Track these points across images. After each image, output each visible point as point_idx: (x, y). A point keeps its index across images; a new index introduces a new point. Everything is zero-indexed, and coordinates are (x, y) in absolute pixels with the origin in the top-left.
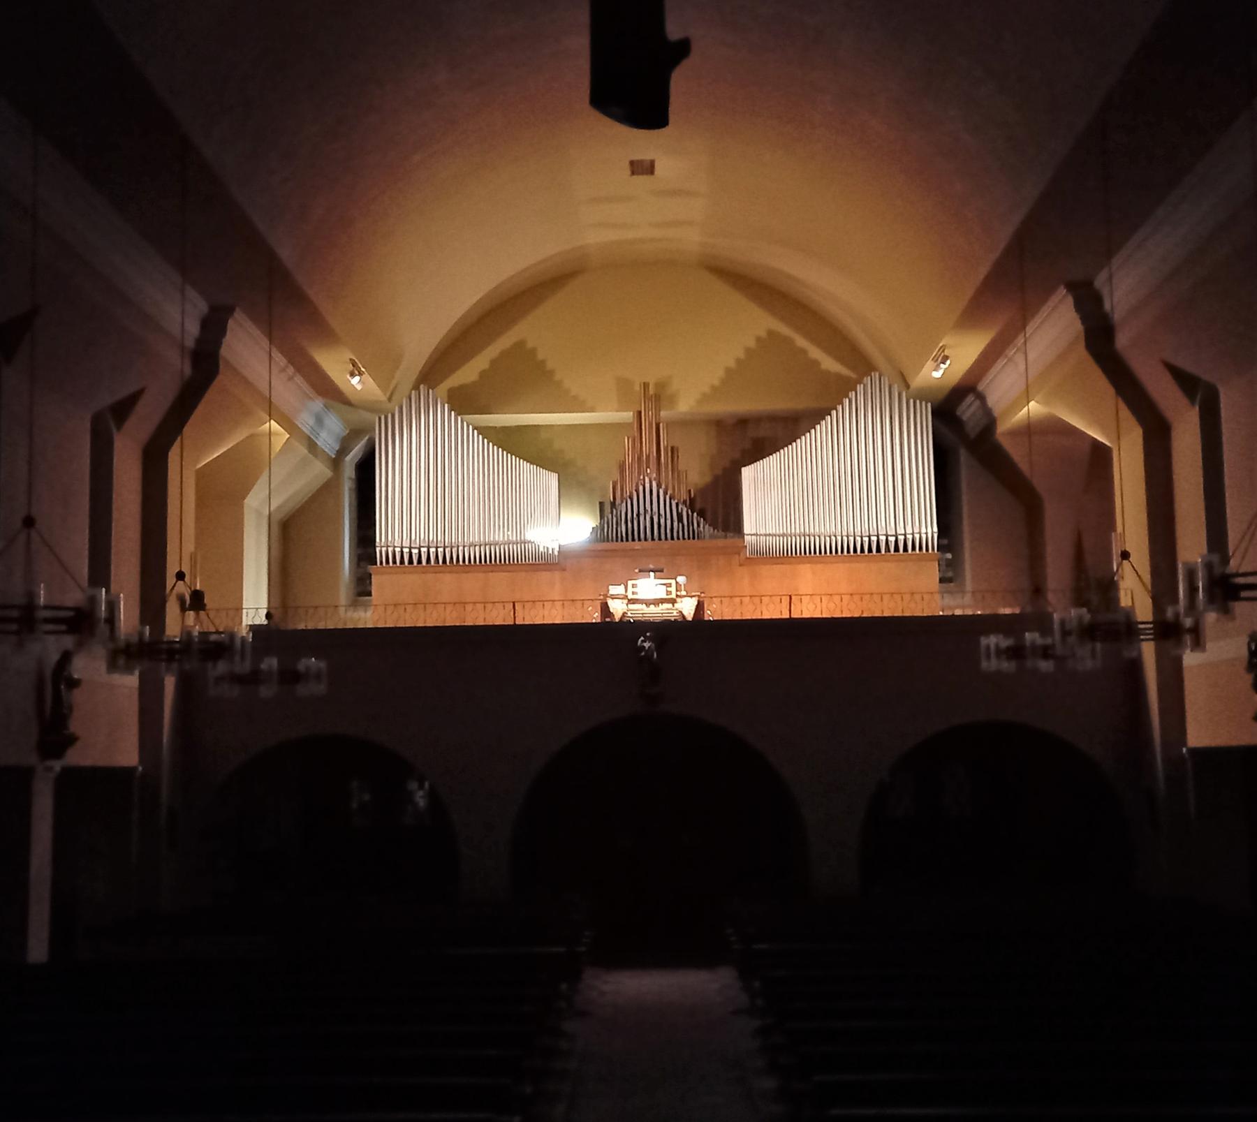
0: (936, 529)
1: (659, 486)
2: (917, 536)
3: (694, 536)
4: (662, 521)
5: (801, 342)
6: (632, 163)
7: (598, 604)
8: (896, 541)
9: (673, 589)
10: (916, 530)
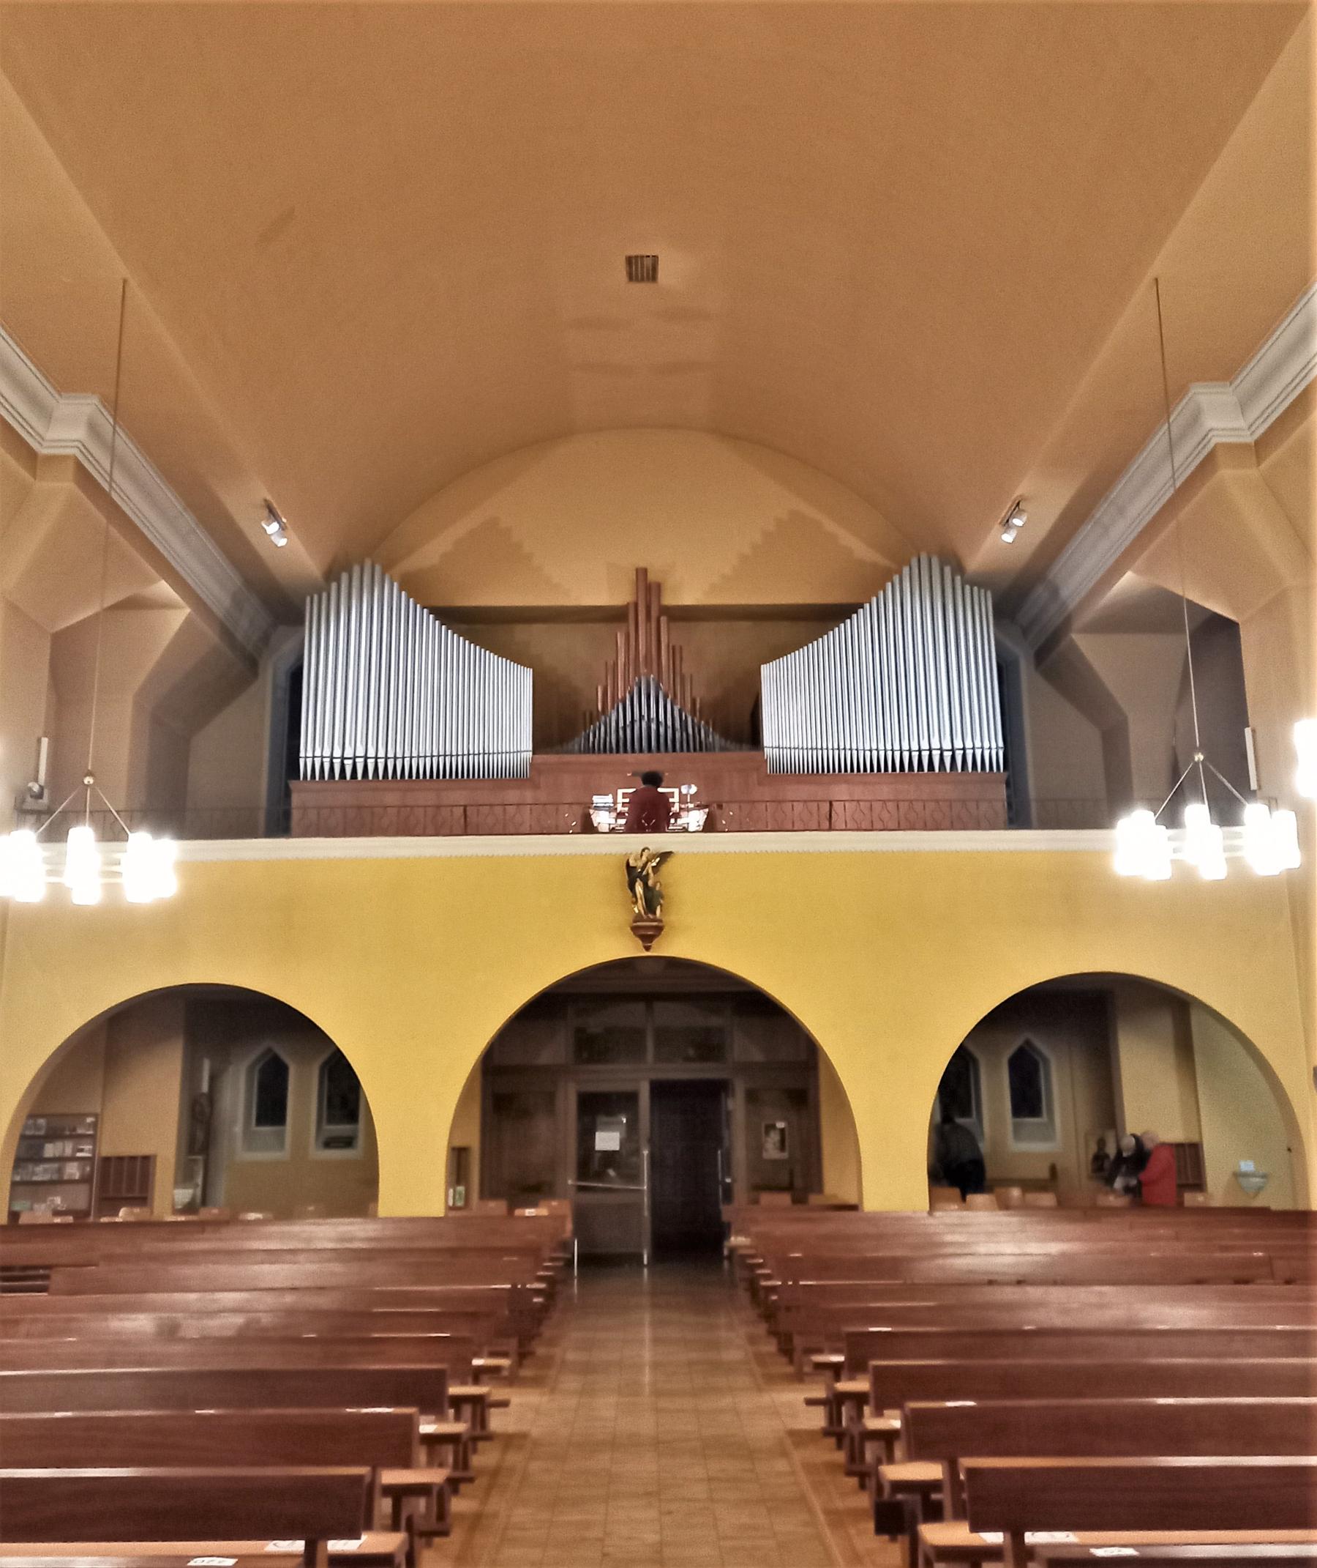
0: (1001, 744)
1: (658, 689)
2: (978, 753)
3: (701, 747)
4: (662, 730)
5: (830, 526)
6: (630, 260)
7: (578, 810)
8: (953, 757)
9: (676, 799)
10: (978, 744)
